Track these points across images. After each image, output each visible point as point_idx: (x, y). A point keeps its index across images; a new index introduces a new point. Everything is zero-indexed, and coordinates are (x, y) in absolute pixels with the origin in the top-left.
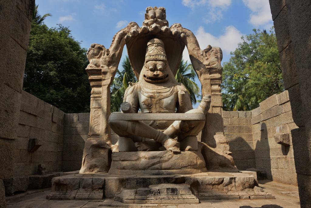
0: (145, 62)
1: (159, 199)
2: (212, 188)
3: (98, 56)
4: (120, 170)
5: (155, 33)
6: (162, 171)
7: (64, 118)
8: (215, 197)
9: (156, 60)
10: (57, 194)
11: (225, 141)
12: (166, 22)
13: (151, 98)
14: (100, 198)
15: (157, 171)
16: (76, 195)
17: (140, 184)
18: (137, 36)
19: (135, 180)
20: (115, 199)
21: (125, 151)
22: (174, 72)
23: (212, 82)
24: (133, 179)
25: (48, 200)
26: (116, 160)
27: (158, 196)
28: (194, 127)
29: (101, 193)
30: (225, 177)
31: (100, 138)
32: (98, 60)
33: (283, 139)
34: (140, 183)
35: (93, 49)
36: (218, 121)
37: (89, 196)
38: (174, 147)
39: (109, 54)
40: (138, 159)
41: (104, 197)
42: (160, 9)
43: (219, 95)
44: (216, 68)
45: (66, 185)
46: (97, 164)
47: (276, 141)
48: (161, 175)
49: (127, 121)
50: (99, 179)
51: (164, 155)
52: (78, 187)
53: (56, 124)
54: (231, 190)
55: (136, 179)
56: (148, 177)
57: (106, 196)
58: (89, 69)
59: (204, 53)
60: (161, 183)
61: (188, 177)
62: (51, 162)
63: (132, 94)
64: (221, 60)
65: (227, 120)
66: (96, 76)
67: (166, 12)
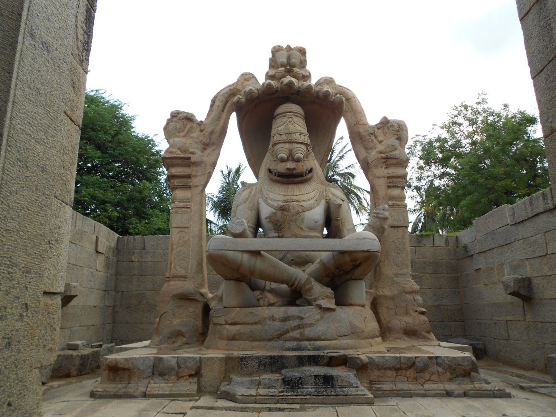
1: (301, 395)
3: (184, 133)
4: (226, 342)
8: (401, 392)
9: (290, 143)
10: (111, 388)
15: (294, 344)
19: (256, 361)
20: (220, 395)
23: (390, 182)
24: (251, 358)
25: (93, 399)
26: (220, 322)
28: (361, 263)
29: (194, 384)
30: (419, 355)
32: (184, 140)
33: (520, 287)
34: (264, 365)
35: (175, 119)
37: (171, 391)
38: (323, 299)
39: (204, 130)
41: (200, 392)
42: (296, 50)
43: (401, 205)
44: (398, 157)
45: (129, 370)
46: (183, 330)
47: (506, 290)
48: (303, 350)
49: (241, 252)
50: (189, 357)
52: (151, 374)
53: (103, 255)
54: (429, 380)
55: (258, 357)
56: (280, 355)
58: (168, 156)
59: (376, 130)
60: (303, 366)
61: (353, 355)
62: (93, 325)
67: (307, 55)
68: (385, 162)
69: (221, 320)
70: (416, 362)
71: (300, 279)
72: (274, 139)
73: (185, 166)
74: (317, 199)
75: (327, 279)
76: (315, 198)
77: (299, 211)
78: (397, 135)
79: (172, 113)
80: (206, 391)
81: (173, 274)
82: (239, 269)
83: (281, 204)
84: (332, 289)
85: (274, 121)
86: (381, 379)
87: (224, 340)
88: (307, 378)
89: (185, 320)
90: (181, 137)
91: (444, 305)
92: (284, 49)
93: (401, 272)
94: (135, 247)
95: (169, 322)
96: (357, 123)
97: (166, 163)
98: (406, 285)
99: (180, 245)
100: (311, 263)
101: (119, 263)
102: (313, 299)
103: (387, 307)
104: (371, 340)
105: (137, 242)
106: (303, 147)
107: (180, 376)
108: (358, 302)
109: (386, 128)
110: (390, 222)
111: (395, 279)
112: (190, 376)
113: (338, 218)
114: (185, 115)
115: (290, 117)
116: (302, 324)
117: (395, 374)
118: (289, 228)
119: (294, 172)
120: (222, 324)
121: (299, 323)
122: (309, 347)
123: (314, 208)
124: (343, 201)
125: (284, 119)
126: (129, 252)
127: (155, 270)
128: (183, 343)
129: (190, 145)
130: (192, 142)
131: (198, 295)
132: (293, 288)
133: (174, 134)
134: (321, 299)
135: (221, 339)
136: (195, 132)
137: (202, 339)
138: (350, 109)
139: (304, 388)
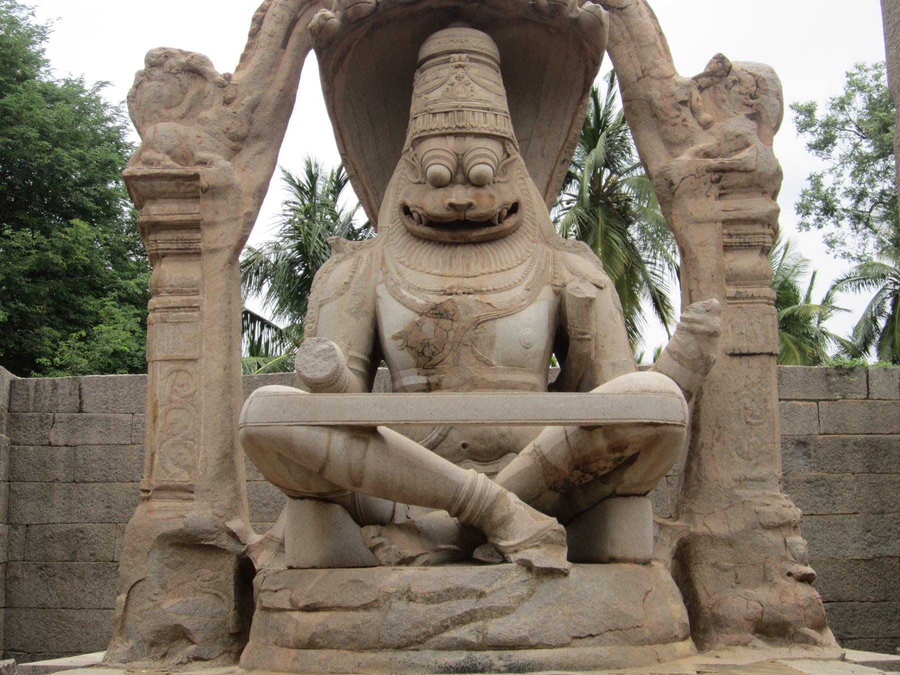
0: (408, 141)
4: (294, 653)
6: (488, 657)
7: (10, 404)
11: (782, 518)
18: (367, 16)
21: (317, 564)
22: (548, 184)
23: (730, 235)
31: (195, 503)
32: (182, 128)
35: (158, 72)
36: (753, 421)
38: (537, 546)
40: (376, 601)
43: (760, 297)
44: (752, 165)
49: (327, 430)
51: (495, 586)
58: (139, 173)
59: (696, 93)
64: (776, 129)
65: (815, 411)
68: (718, 181)
69: (281, 600)
71: (481, 495)
72: (418, 125)
73: (185, 198)
74: (529, 283)
78: (751, 106)
81: (158, 481)
82: (322, 470)
83: (436, 299)
84: (560, 522)
85: (417, 74)
87: (288, 647)
89: (191, 599)
90: (175, 121)
91: (891, 557)
93: (754, 474)
94: (56, 405)
95: (151, 604)
96: (645, 73)
97: (136, 190)
98: (765, 509)
99: (174, 405)
100: (513, 454)
101: (16, 448)
102: (512, 546)
103: (714, 565)
104: (659, 648)
105: (61, 391)
106: (494, 147)
108: (631, 554)
109: (721, 86)
110: (727, 341)
111: (738, 492)
113: (584, 334)
114: (183, 60)
115: (460, 66)
118: (456, 363)
119: (470, 213)
120: (284, 610)
122: (499, 664)
123: (521, 308)
124: (601, 288)
125: (445, 71)
126: (41, 420)
127: (110, 469)
128: (189, 659)
129: (198, 140)
130: (203, 134)
131: (225, 535)
132: (465, 516)
133: (155, 112)
134: (531, 547)
135: (282, 646)
136: (211, 106)
137: (235, 648)
138: (627, 35)
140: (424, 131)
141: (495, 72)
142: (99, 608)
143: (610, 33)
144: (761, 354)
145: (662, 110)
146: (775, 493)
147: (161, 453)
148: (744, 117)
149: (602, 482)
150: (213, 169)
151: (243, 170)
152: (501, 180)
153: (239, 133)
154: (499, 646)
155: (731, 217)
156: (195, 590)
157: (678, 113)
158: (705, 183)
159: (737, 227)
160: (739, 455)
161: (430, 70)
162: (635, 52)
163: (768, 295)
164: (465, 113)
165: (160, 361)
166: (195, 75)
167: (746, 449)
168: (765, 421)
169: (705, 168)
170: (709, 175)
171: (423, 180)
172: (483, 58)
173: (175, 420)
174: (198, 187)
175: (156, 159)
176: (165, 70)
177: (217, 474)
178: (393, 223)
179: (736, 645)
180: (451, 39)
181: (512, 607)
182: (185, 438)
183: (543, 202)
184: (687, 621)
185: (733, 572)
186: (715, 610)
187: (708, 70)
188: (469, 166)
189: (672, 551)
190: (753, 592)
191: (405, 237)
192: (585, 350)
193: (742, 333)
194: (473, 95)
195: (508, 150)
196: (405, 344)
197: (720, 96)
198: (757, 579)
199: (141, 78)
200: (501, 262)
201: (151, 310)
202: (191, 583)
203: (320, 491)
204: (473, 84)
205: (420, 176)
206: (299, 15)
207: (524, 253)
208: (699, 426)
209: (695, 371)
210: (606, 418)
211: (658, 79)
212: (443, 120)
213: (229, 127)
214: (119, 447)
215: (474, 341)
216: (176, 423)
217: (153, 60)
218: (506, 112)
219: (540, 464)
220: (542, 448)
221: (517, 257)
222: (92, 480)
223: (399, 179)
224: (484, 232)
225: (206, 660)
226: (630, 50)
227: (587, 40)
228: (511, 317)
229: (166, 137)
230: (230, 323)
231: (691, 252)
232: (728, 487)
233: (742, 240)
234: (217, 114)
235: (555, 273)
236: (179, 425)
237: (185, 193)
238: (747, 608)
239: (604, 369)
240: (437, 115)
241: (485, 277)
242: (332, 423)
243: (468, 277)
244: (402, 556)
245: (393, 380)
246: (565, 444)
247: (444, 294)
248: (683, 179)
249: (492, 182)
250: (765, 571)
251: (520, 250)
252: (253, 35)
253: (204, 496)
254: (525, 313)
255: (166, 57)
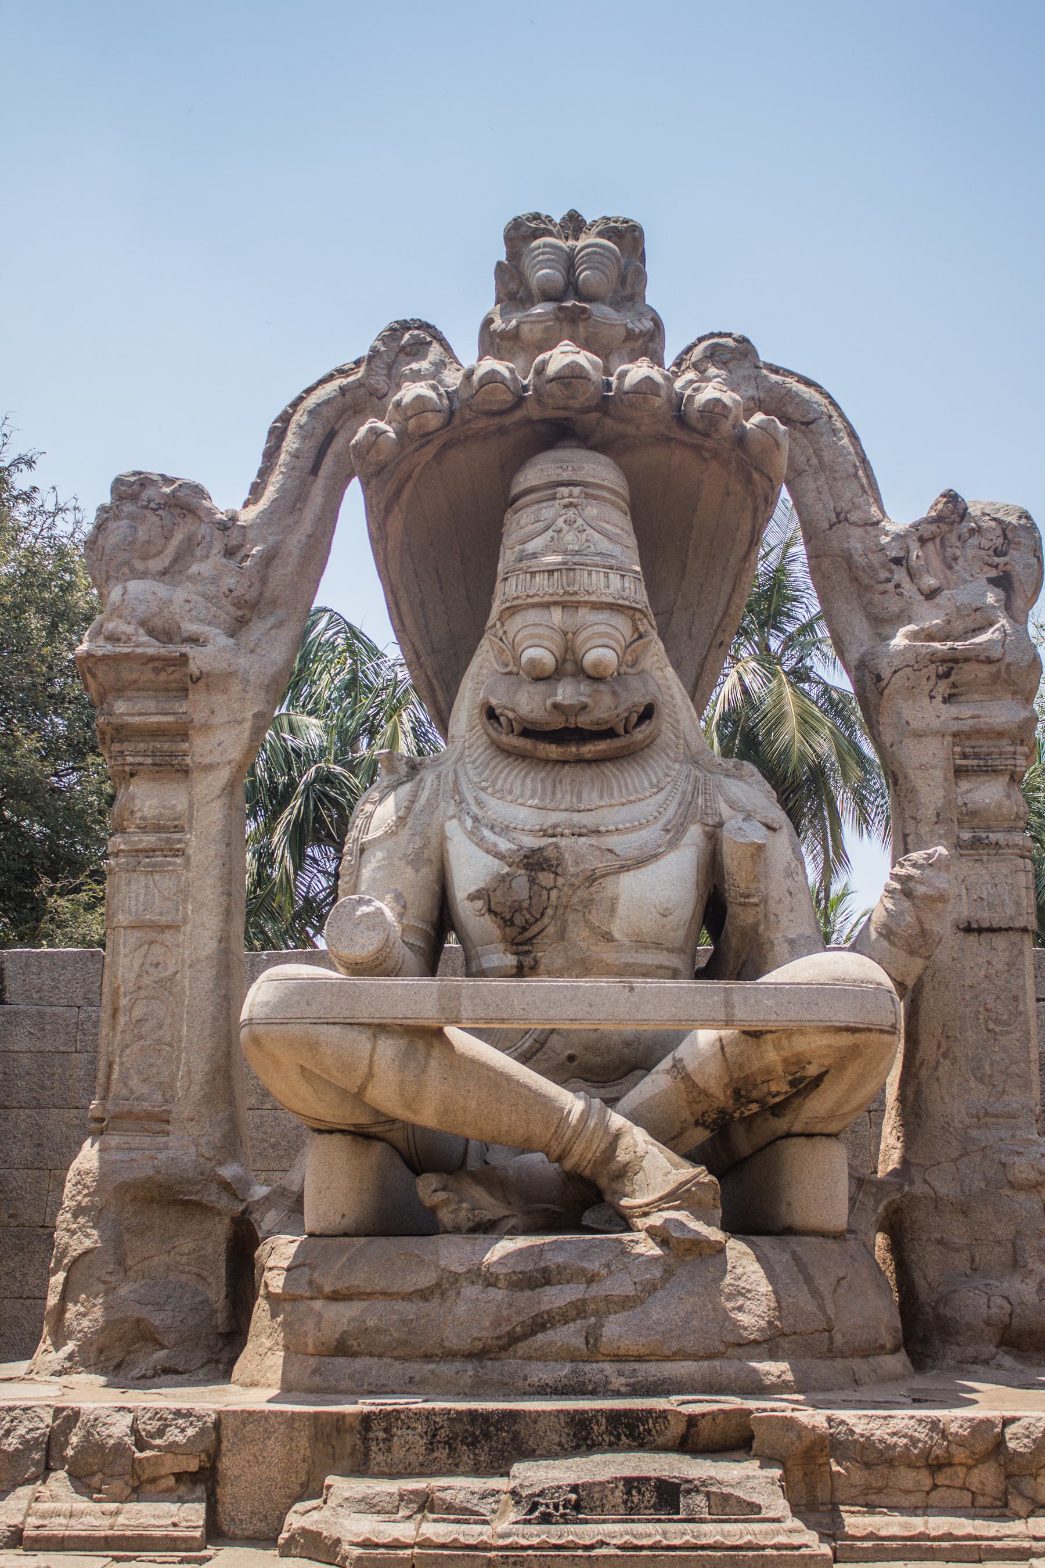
2: (927, 1482)
4: (312, 1362)
5: (565, 409)
6: (602, 1371)
11: (1041, 1173)
12: (648, 325)
13: (527, 867)
14: (185, 1539)
15: (563, 1370)
16: (27, 1515)
17: (450, 1448)
22: (699, 677)
23: (965, 756)
27: (571, 1527)
28: (826, 1072)
31: (171, 1137)
32: (162, 590)
35: (128, 508)
36: (997, 1029)
40: (438, 1285)
42: (600, 234)
44: (996, 654)
46: (157, 1319)
52: (42, 1469)
57: (225, 1528)
63: (404, 834)
66: (151, 705)
67: (648, 246)
70: (1007, 1437)
73: (167, 690)
74: (669, 821)
75: (700, 1136)
76: (663, 820)
77: (598, 873)
78: (996, 566)
79: (118, 482)
80: (238, 1532)
82: (362, 1088)
83: (531, 842)
84: (710, 1172)
85: (508, 515)
86: (874, 1497)
88: (598, 1488)
92: (555, 230)
99: (143, 993)
102: (640, 1207)
103: (940, 1242)
107: (145, 1477)
111: (974, 1133)
112: (179, 1477)
113: (748, 896)
114: (167, 490)
115: (571, 504)
116: (593, 1298)
117: (927, 1482)
118: (562, 935)
121: (580, 1297)
122: (617, 1382)
123: (655, 857)
125: (548, 512)
127: (43, 1088)
128: (155, 1369)
129: (187, 607)
130: (195, 598)
131: (214, 1187)
136: (207, 557)
137: (225, 1356)
139: (586, 1522)
140: (517, 598)
141: (622, 514)
142: (21, 1297)
143: (789, 458)
144: (1010, 929)
145: (864, 570)
146: (1030, 1136)
147: (122, 1063)
148: (985, 582)
149: (773, 1115)
150: (210, 647)
151: (252, 651)
152: (630, 670)
153: (247, 597)
154: (618, 1358)
155: (966, 728)
156: (168, 1268)
157: (888, 575)
158: (928, 679)
159: (973, 742)
160: (976, 1078)
161: (529, 510)
162: (826, 487)
163: (1021, 843)
164: (578, 572)
165: (124, 928)
166: (184, 511)
167: (988, 1070)
168: (1016, 1028)
169: (928, 657)
170: (934, 666)
171: (515, 670)
172: (605, 494)
173: (145, 1014)
174: (186, 675)
175: (124, 633)
176: (140, 504)
177: (204, 1096)
178: (471, 731)
179: (972, 1363)
180: (559, 465)
181: (639, 1297)
182: (159, 1041)
183: (690, 704)
184: (900, 1326)
185: (967, 1252)
186: (942, 1310)
187: (933, 514)
188: (583, 650)
189: (877, 1220)
190: (998, 1284)
191: (487, 752)
192: (751, 921)
193: (982, 899)
194: (589, 547)
195: (640, 627)
196: (487, 906)
197: (949, 551)
198: (1003, 1264)
199: (106, 515)
200: (627, 790)
201: (113, 853)
202: (162, 1257)
203: (356, 1122)
204: (589, 531)
205: (512, 663)
206: (337, 427)
207: (660, 774)
208: (917, 1032)
209: (912, 953)
210: (779, 1018)
211: (859, 526)
212: (546, 582)
213: (232, 587)
214: (57, 1056)
215: (588, 904)
216: (146, 1020)
217: (123, 488)
218: (636, 572)
219: (682, 1086)
220: (685, 1062)
221: (651, 783)
222: (15, 1104)
223: (481, 668)
224: (602, 746)
225: (181, 1373)
226: (819, 483)
227: (756, 469)
228: (643, 870)
229: (140, 601)
230: (230, 873)
231: (906, 778)
232: (961, 1126)
233: (982, 763)
234: (215, 568)
235: (706, 806)
236: (152, 1022)
237: (166, 682)
238: (989, 1307)
239: (777, 948)
240: (537, 575)
241: (605, 811)
242: (378, 1021)
243: (579, 811)
244: (477, 1220)
245: (468, 961)
246: (720, 1057)
247: (544, 836)
248: (895, 672)
249: (616, 674)
250: (1014, 1251)
251: (656, 773)
252: (270, 455)
253: (185, 1128)
254: (662, 862)
255: (142, 485)
